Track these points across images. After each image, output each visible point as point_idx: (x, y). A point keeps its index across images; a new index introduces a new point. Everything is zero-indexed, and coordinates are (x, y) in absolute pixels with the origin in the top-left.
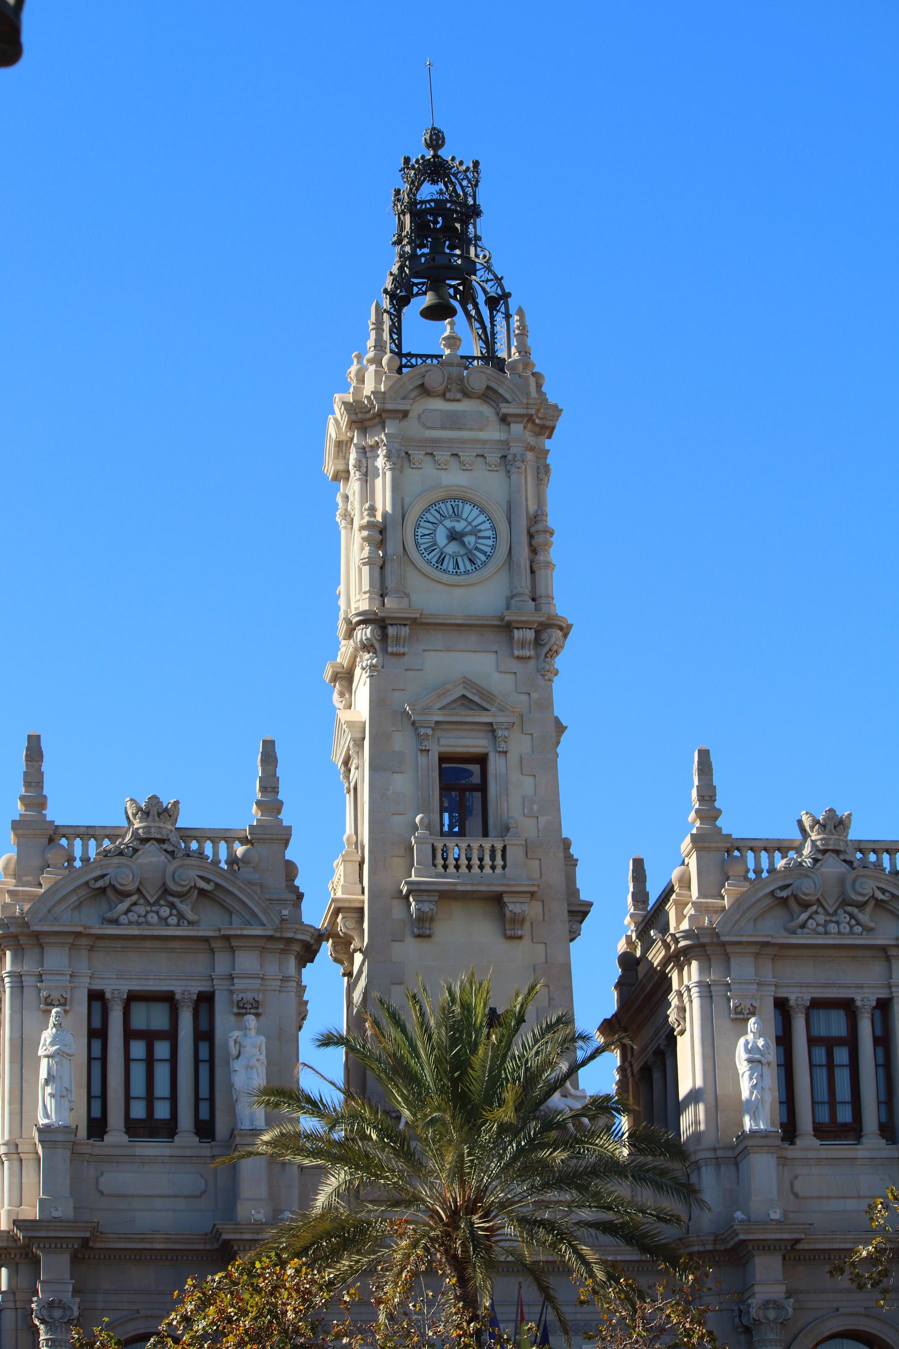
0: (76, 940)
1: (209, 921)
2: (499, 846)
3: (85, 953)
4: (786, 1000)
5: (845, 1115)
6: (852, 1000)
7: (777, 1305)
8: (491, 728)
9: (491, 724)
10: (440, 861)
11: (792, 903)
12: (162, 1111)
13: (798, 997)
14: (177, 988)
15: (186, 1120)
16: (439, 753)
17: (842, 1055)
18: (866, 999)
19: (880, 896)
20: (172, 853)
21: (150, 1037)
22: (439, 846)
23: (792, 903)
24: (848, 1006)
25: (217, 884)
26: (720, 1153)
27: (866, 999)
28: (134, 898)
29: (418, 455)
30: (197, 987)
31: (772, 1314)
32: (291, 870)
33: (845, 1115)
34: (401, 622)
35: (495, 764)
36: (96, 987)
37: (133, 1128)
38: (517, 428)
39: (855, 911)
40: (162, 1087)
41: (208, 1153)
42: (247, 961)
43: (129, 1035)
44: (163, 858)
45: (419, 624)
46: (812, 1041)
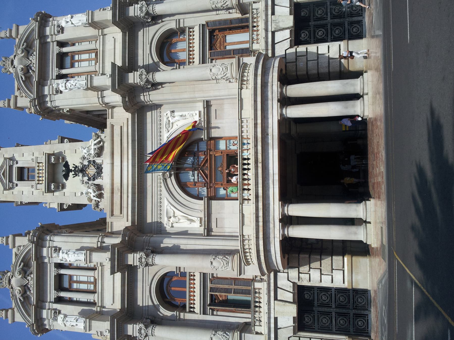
1: (34, 263)
2: (37, 164)
3: (43, 304)
4: (57, 76)
5: (93, 55)
6: (57, 54)
7: (141, 75)
9: (9, 166)
10: (41, 182)
11: (28, 75)
14: (53, 274)
15: (91, 273)
16: (18, 180)
19: (24, 46)
20: (12, 276)
22: (37, 182)
23: (28, 75)
24: (61, 57)
25: (22, 261)
26: (100, 96)
28: (26, 288)
30: (53, 268)
31: (144, 77)
35: (20, 165)
36: (53, 300)
39: (30, 54)
40: (85, 279)
41: (100, 268)
42: (45, 252)
44: (14, 278)
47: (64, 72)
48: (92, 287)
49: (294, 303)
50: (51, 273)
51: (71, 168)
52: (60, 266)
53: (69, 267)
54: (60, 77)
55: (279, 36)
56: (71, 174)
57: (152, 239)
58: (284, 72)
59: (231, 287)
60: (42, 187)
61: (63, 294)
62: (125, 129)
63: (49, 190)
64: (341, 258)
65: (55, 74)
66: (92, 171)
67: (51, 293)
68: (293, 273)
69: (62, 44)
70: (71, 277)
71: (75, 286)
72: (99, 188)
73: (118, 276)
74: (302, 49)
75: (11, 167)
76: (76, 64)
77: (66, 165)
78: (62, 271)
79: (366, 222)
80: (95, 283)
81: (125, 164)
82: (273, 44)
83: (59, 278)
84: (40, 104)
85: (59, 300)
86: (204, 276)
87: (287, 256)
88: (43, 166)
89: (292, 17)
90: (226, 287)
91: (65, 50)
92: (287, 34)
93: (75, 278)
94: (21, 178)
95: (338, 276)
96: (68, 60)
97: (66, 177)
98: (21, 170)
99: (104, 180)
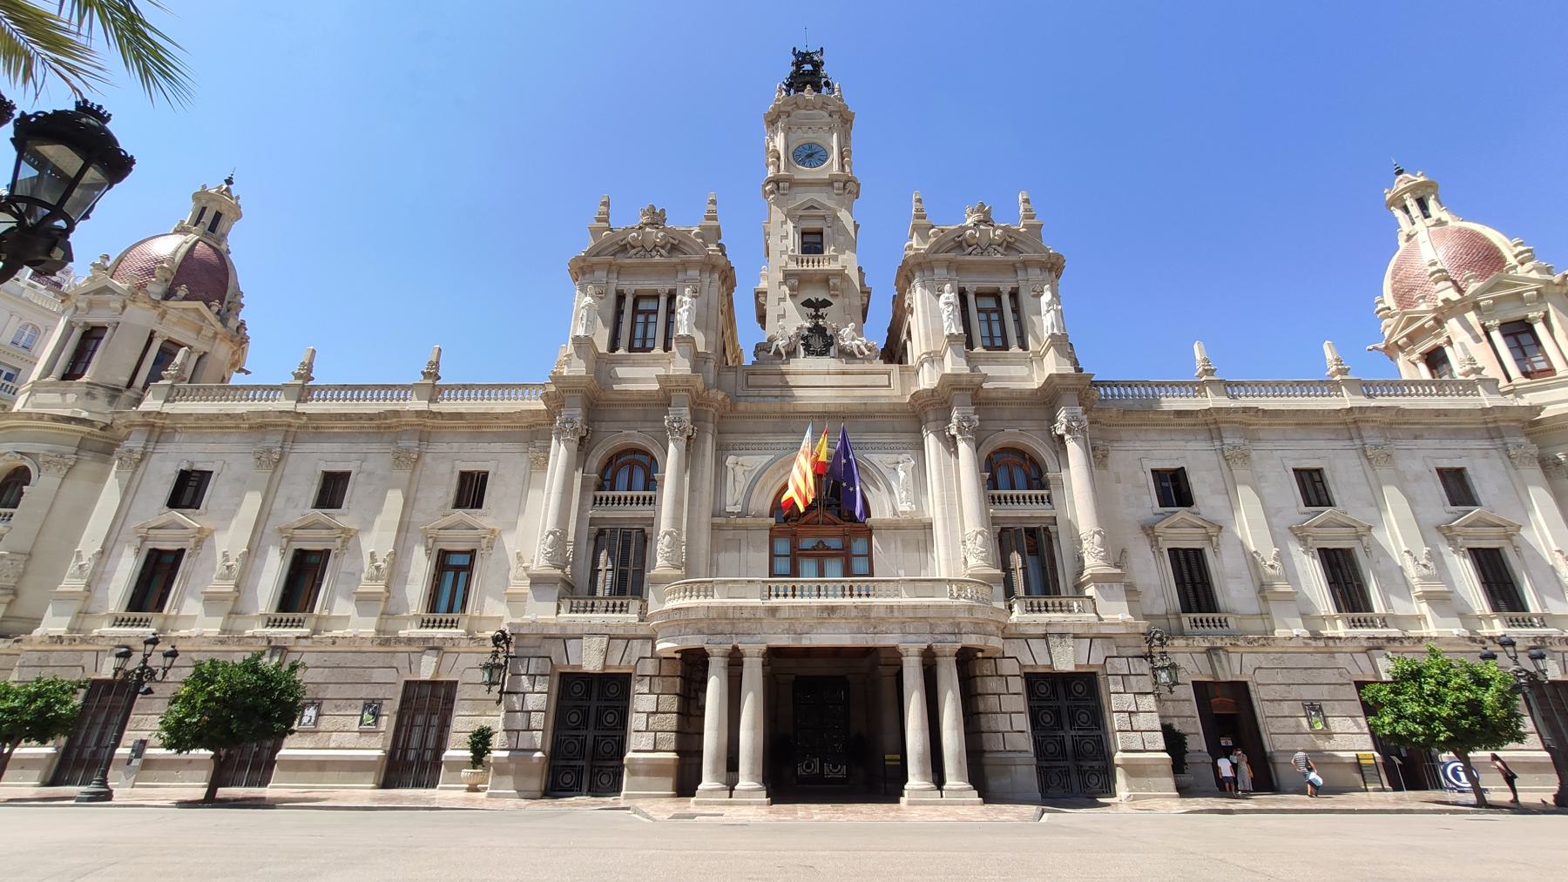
0: (609, 268)
8: (824, 218)
12: (649, 345)
13: (971, 287)
17: (994, 316)
18: (1005, 288)
21: (648, 313)
27: (1005, 288)
29: (794, 128)
32: (722, 248)
33: (998, 342)
34: (785, 180)
37: (631, 349)
38: (836, 117)
43: (636, 311)
45: (793, 183)
46: (979, 311)
47: (971, 298)
48: (637, 344)
49: (605, 666)
50: (661, 286)
51: (822, 311)
52: (671, 297)
53: (671, 312)
54: (963, 295)
55: (1037, 645)
56: (812, 311)
57: (709, 437)
58: (980, 655)
59: (631, 564)
60: (793, 266)
61: (629, 300)
62: (883, 392)
63: (788, 275)
64: (673, 746)
65: (968, 286)
66: (817, 343)
67: (630, 286)
68: (649, 667)
69: (1014, 295)
70: (655, 312)
71: (641, 318)
72: (792, 353)
73: (656, 387)
74: (1018, 685)
75: (824, 218)
76: (983, 316)
77: (826, 304)
78: (663, 300)
79: (732, 789)
80: (644, 349)
81: (829, 392)
82: (1026, 638)
83: (656, 297)
84: (919, 264)
85: (621, 297)
86: (651, 522)
87: (678, 656)
88: (826, 266)
89: (1071, 668)
90: (632, 557)
91: (1006, 299)
92: (1043, 660)
93: (652, 318)
94: (804, 234)
95: (646, 741)
96: (990, 303)
97: (808, 303)
98: (821, 233)
99: (802, 363)
